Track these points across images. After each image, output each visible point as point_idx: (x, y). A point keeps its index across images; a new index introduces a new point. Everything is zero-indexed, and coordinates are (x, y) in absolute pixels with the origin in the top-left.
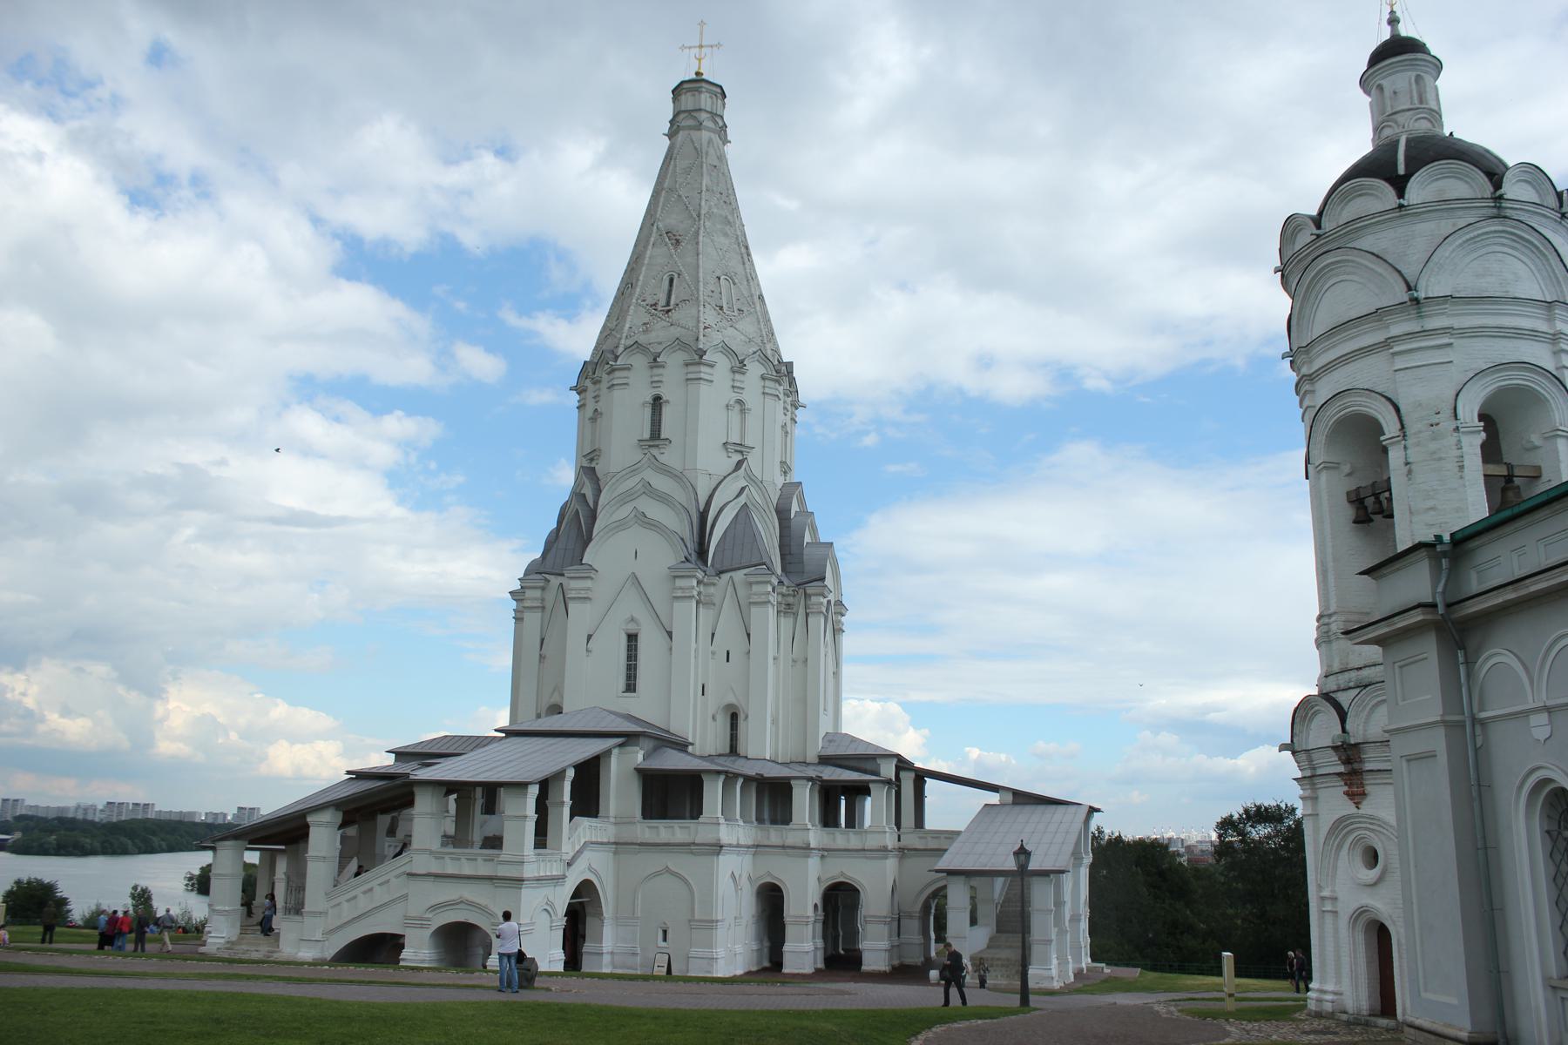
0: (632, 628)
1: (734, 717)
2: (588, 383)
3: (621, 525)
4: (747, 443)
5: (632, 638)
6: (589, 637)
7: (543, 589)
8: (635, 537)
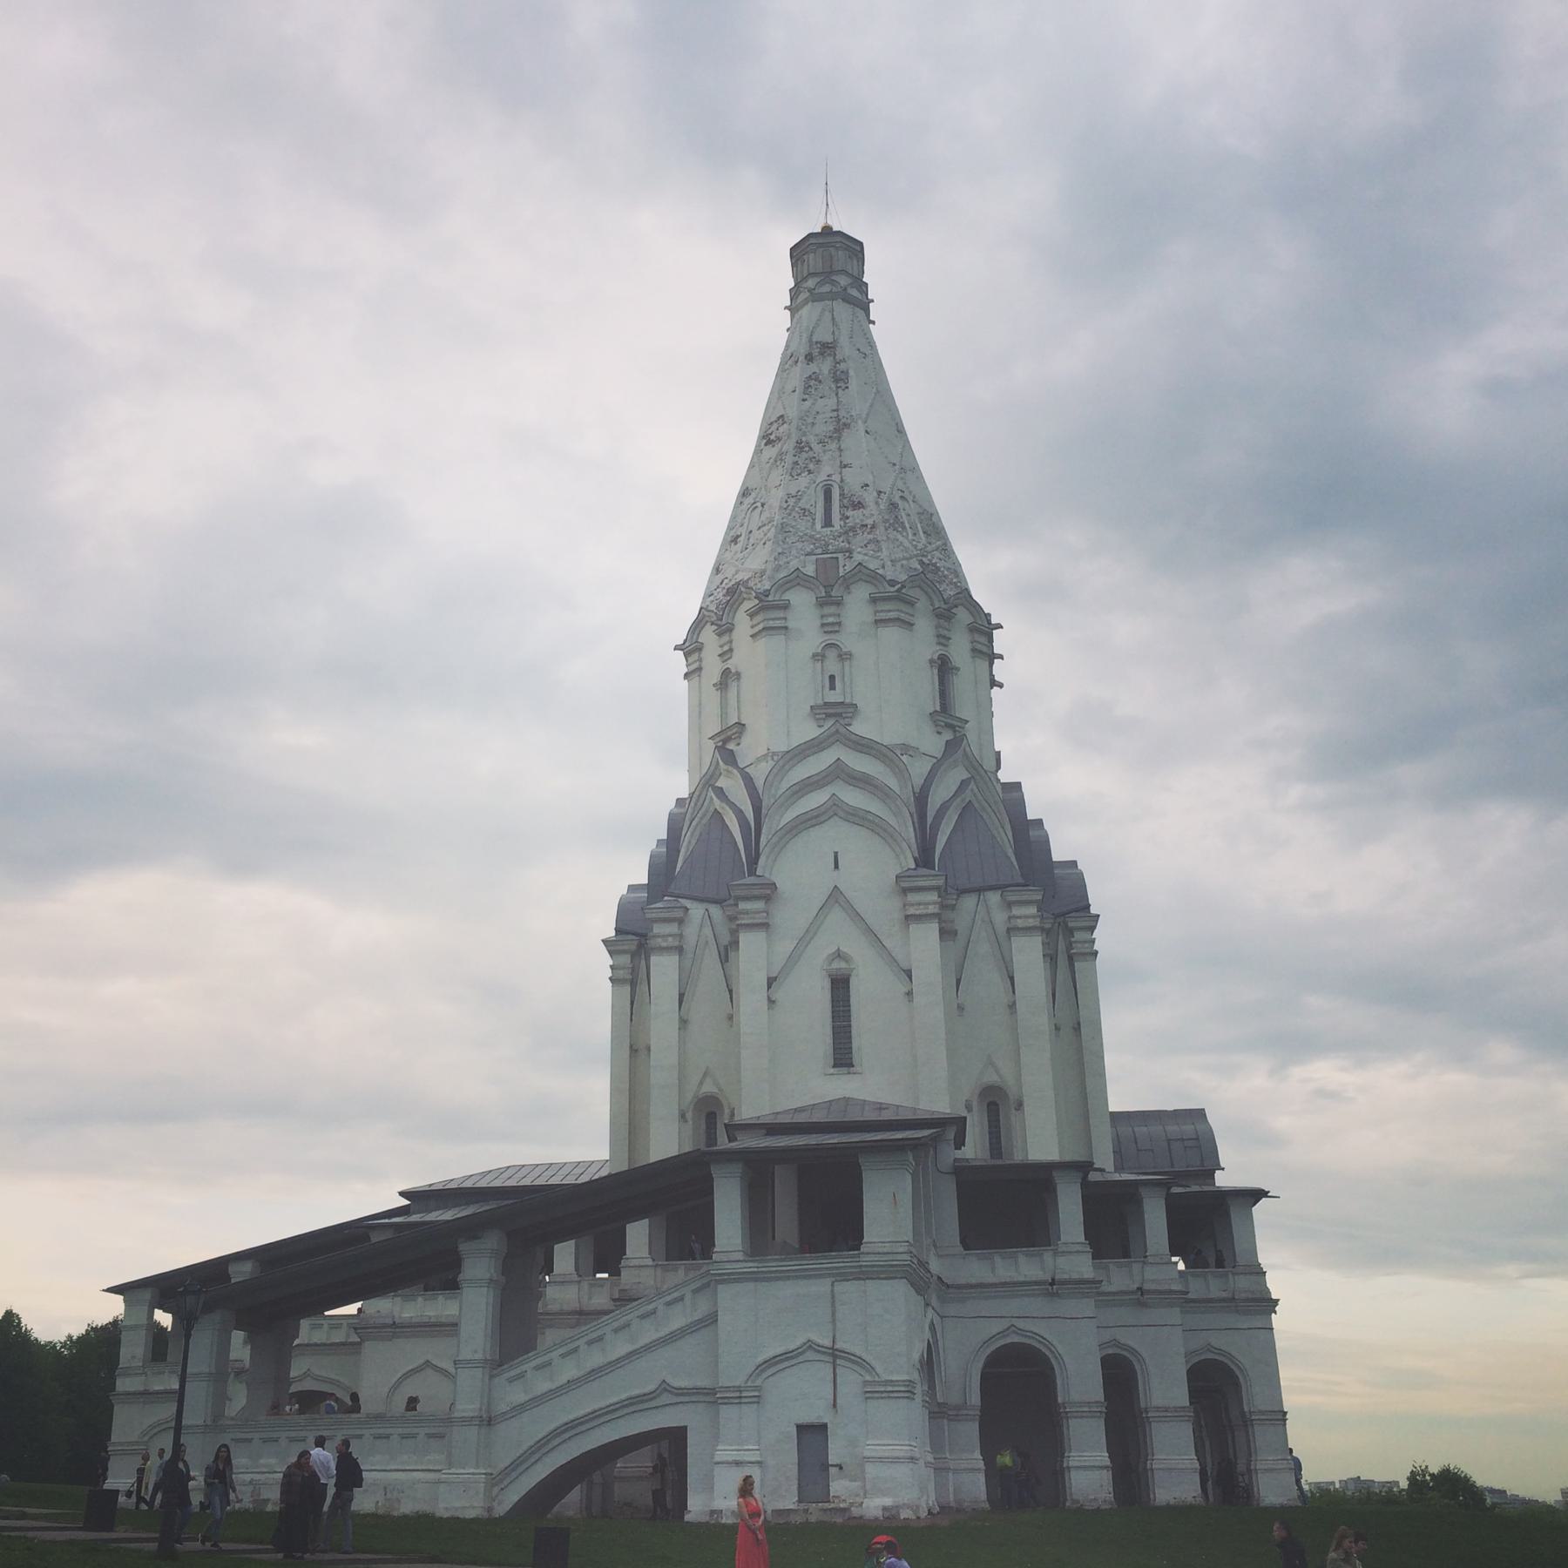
5: (840, 986)
6: (771, 982)
8: (835, 835)
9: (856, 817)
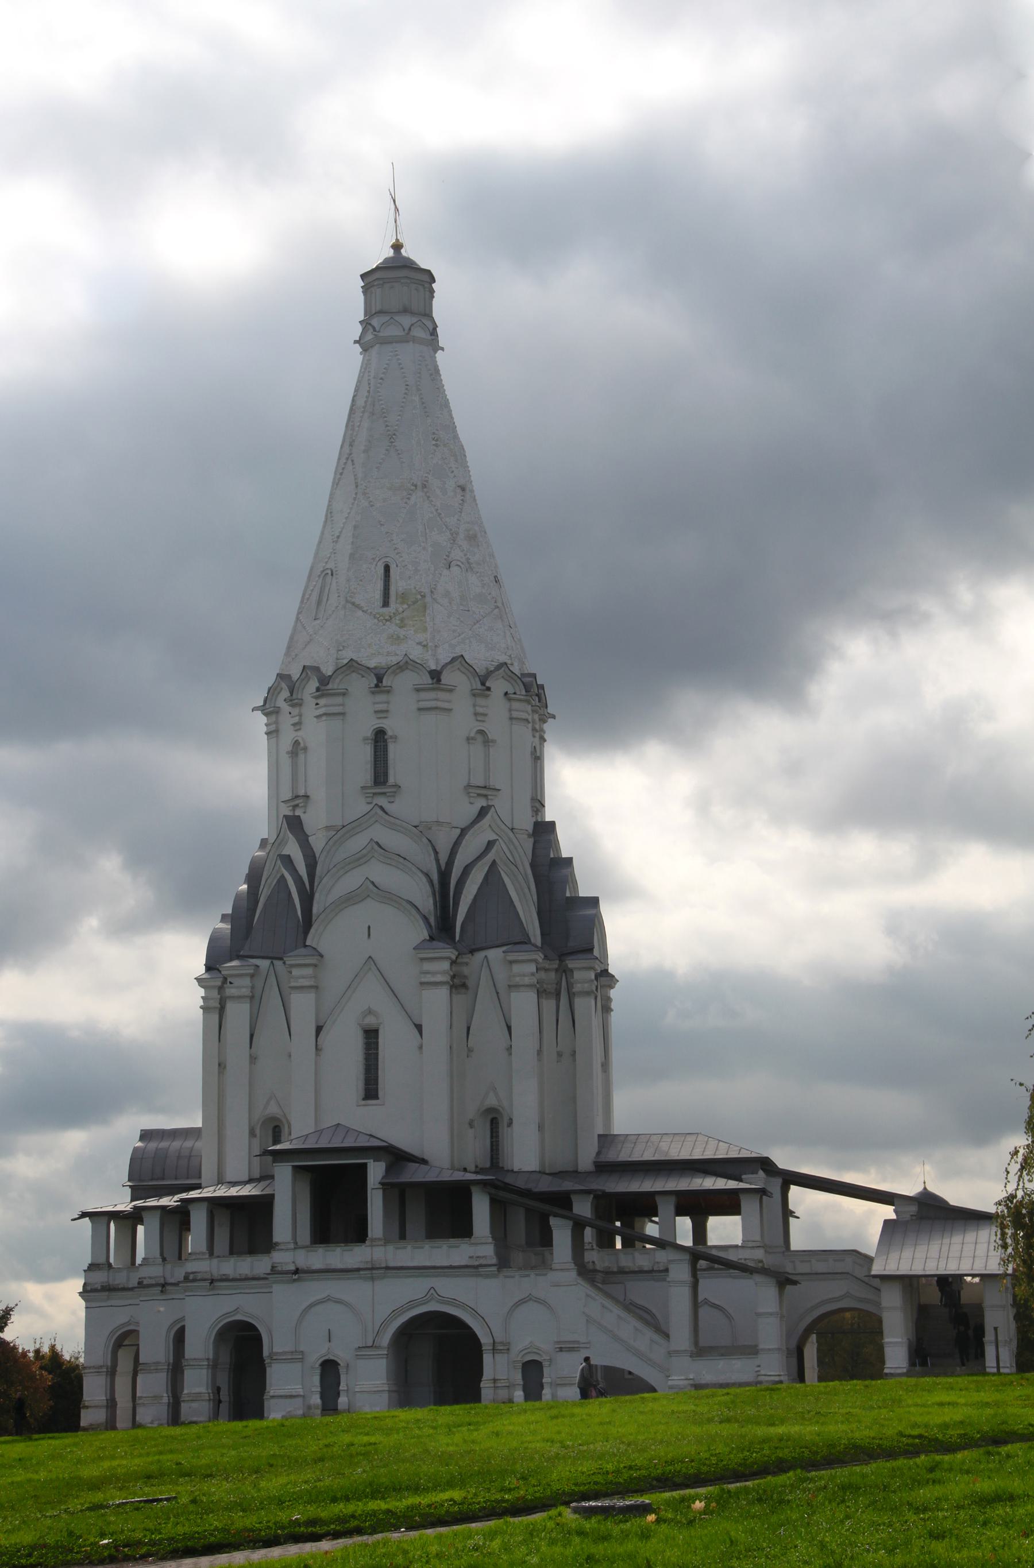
0: (370, 1021)
1: (494, 1124)
3: (351, 899)
4: (493, 782)
5: (371, 1036)
7: (252, 976)
9: (387, 897)
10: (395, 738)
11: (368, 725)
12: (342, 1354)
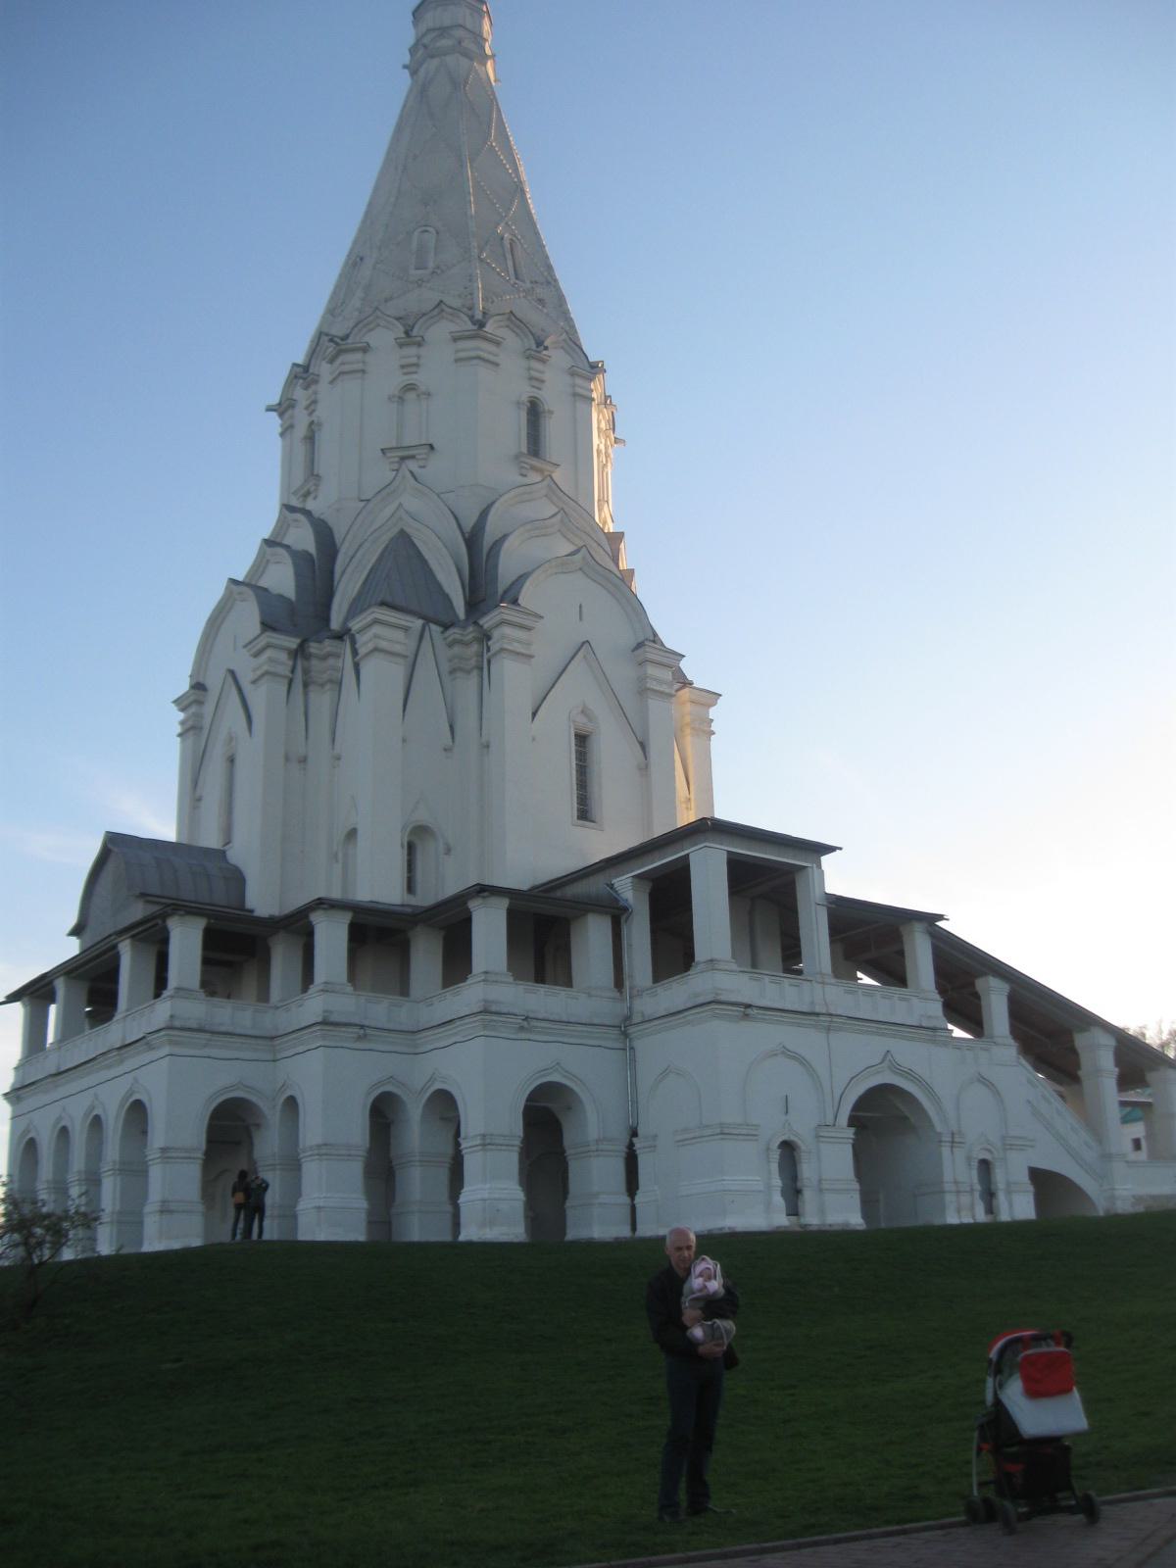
2: (383, 339)
10: (551, 412)
11: (526, 391)
12: (802, 1130)
